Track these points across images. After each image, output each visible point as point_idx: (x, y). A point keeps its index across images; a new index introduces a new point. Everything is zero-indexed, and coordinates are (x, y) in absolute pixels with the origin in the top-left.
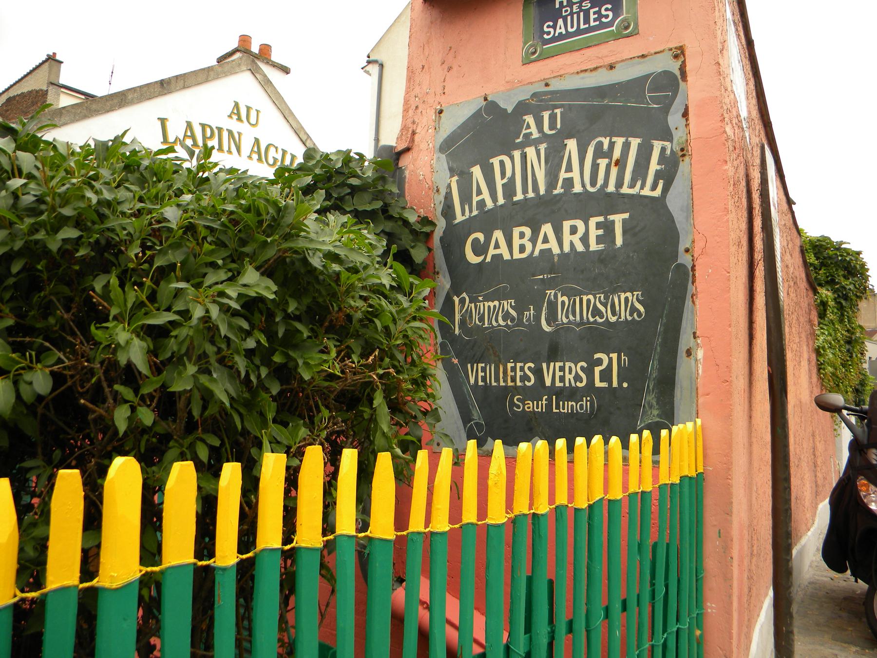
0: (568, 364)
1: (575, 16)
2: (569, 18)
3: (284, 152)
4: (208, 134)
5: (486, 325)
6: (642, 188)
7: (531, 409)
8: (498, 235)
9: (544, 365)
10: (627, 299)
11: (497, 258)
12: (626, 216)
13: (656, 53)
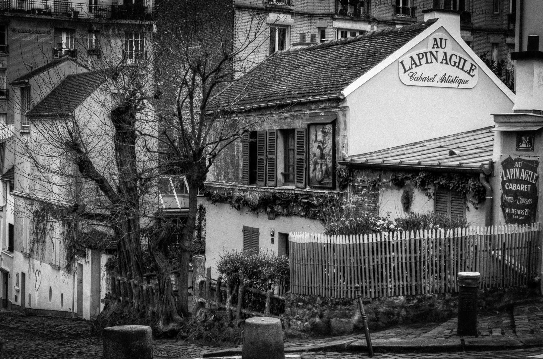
8: (511, 184)
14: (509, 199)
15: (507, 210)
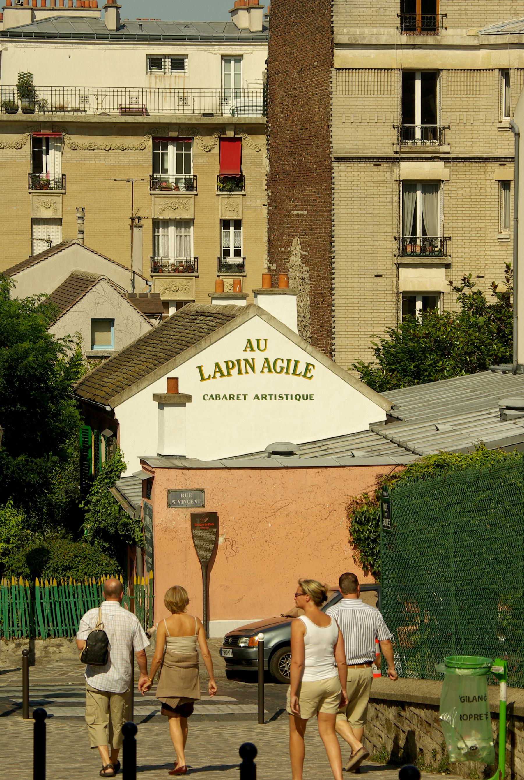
3: (289, 361)
4: (230, 365)
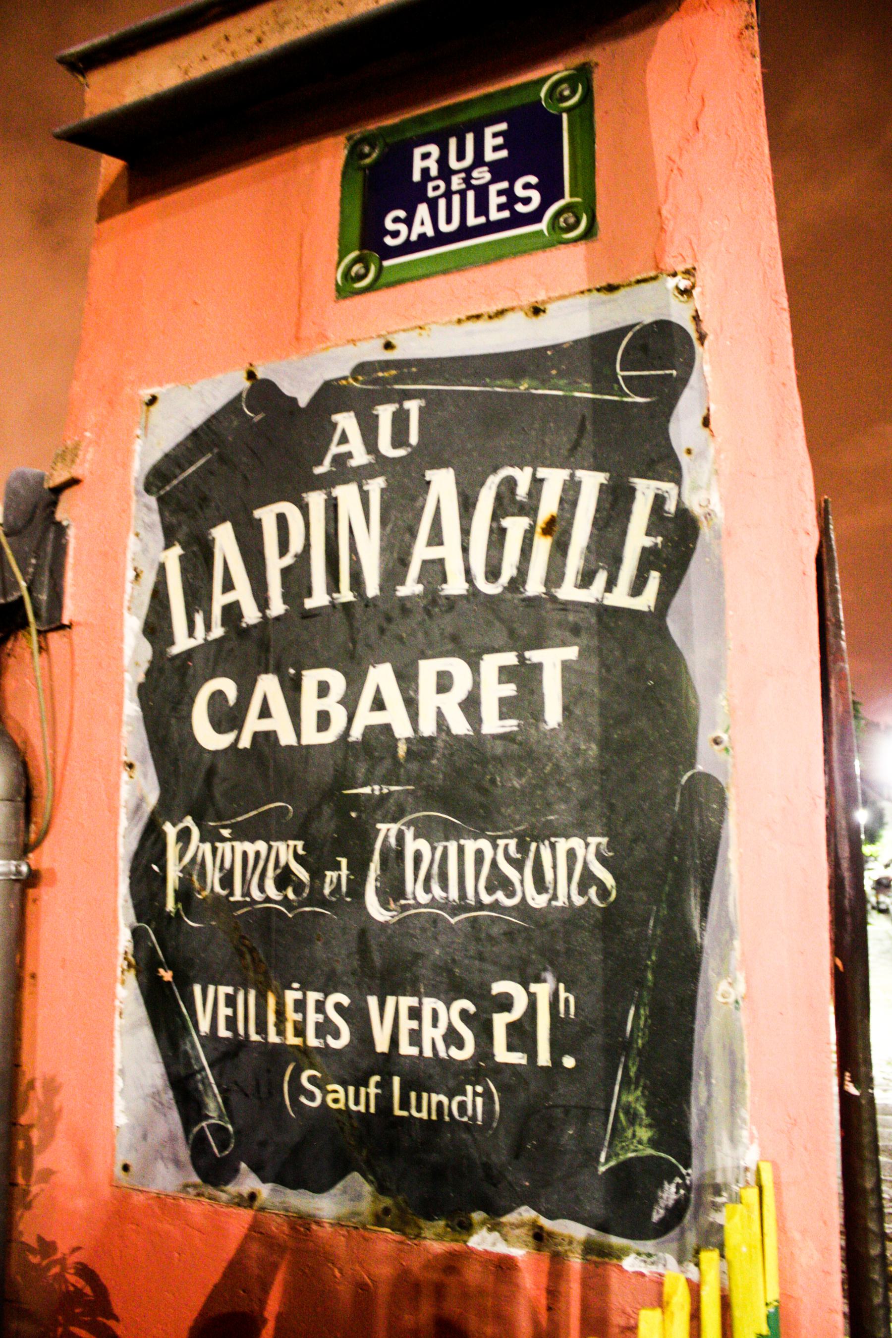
0: (429, 1004)
1: (456, 199)
2: (442, 203)
5: (237, 897)
6: (610, 585)
7: (341, 1105)
8: (268, 685)
9: (373, 1002)
10: (571, 855)
11: (265, 739)
12: (571, 653)
13: (638, 282)
14: (248, 866)
15: (213, 1009)
